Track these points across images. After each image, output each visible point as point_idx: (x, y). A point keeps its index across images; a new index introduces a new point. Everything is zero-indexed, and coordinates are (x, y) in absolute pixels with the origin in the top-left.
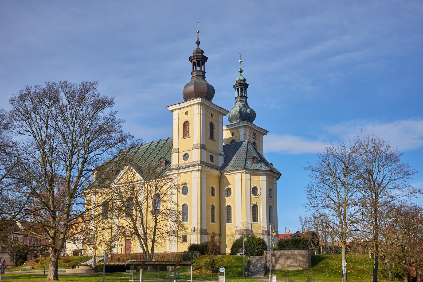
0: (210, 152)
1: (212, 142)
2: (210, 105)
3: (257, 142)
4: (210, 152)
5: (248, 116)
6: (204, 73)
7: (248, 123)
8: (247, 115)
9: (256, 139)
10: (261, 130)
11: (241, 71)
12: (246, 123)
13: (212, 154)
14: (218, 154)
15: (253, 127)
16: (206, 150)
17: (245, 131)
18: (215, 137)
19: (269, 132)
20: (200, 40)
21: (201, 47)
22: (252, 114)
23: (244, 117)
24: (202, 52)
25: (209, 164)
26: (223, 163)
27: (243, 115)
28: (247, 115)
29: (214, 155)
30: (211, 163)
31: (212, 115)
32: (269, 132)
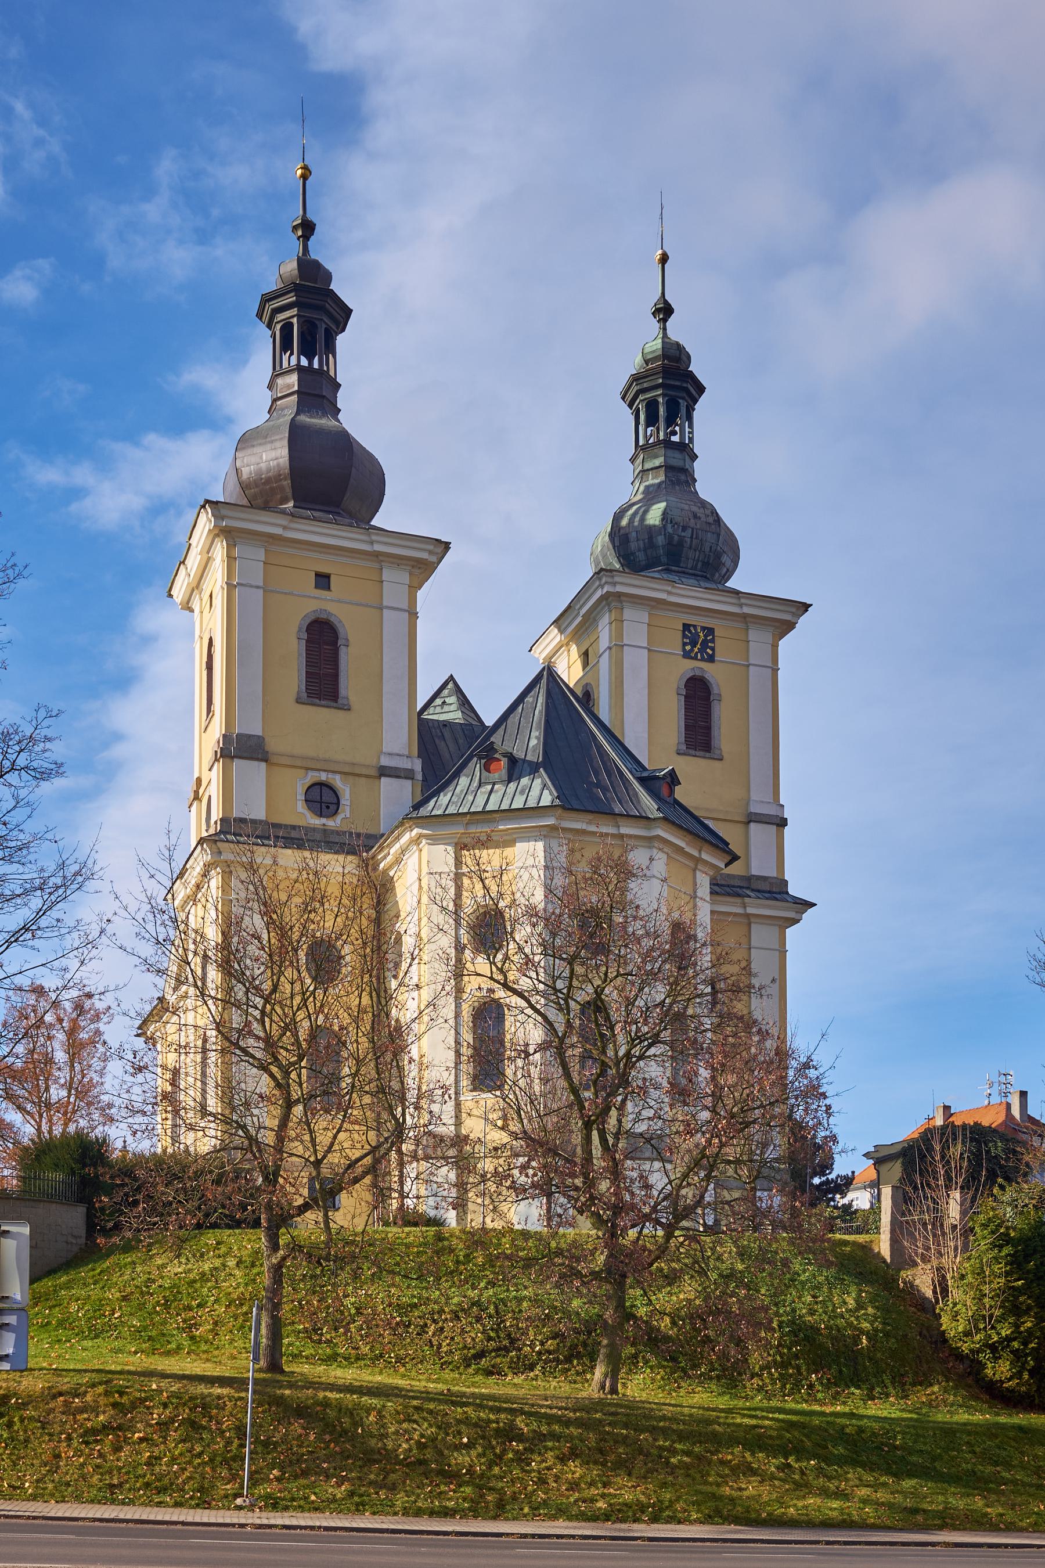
0: (307, 769)
1: (322, 715)
3: (712, 672)
4: (307, 769)
5: (660, 540)
8: (650, 538)
9: (711, 659)
10: (741, 606)
13: (323, 777)
14: (373, 772)
15: (669, 593)
16: (266, 760)
18: (351, 684)
19: (806, 607)
22: (684, 529)
23: (641, 556)
25: (294, 827)
27: (633, 546)
28: (650, 538)
29: (337, 781)
30: (316, 821)
32: (806, 607)
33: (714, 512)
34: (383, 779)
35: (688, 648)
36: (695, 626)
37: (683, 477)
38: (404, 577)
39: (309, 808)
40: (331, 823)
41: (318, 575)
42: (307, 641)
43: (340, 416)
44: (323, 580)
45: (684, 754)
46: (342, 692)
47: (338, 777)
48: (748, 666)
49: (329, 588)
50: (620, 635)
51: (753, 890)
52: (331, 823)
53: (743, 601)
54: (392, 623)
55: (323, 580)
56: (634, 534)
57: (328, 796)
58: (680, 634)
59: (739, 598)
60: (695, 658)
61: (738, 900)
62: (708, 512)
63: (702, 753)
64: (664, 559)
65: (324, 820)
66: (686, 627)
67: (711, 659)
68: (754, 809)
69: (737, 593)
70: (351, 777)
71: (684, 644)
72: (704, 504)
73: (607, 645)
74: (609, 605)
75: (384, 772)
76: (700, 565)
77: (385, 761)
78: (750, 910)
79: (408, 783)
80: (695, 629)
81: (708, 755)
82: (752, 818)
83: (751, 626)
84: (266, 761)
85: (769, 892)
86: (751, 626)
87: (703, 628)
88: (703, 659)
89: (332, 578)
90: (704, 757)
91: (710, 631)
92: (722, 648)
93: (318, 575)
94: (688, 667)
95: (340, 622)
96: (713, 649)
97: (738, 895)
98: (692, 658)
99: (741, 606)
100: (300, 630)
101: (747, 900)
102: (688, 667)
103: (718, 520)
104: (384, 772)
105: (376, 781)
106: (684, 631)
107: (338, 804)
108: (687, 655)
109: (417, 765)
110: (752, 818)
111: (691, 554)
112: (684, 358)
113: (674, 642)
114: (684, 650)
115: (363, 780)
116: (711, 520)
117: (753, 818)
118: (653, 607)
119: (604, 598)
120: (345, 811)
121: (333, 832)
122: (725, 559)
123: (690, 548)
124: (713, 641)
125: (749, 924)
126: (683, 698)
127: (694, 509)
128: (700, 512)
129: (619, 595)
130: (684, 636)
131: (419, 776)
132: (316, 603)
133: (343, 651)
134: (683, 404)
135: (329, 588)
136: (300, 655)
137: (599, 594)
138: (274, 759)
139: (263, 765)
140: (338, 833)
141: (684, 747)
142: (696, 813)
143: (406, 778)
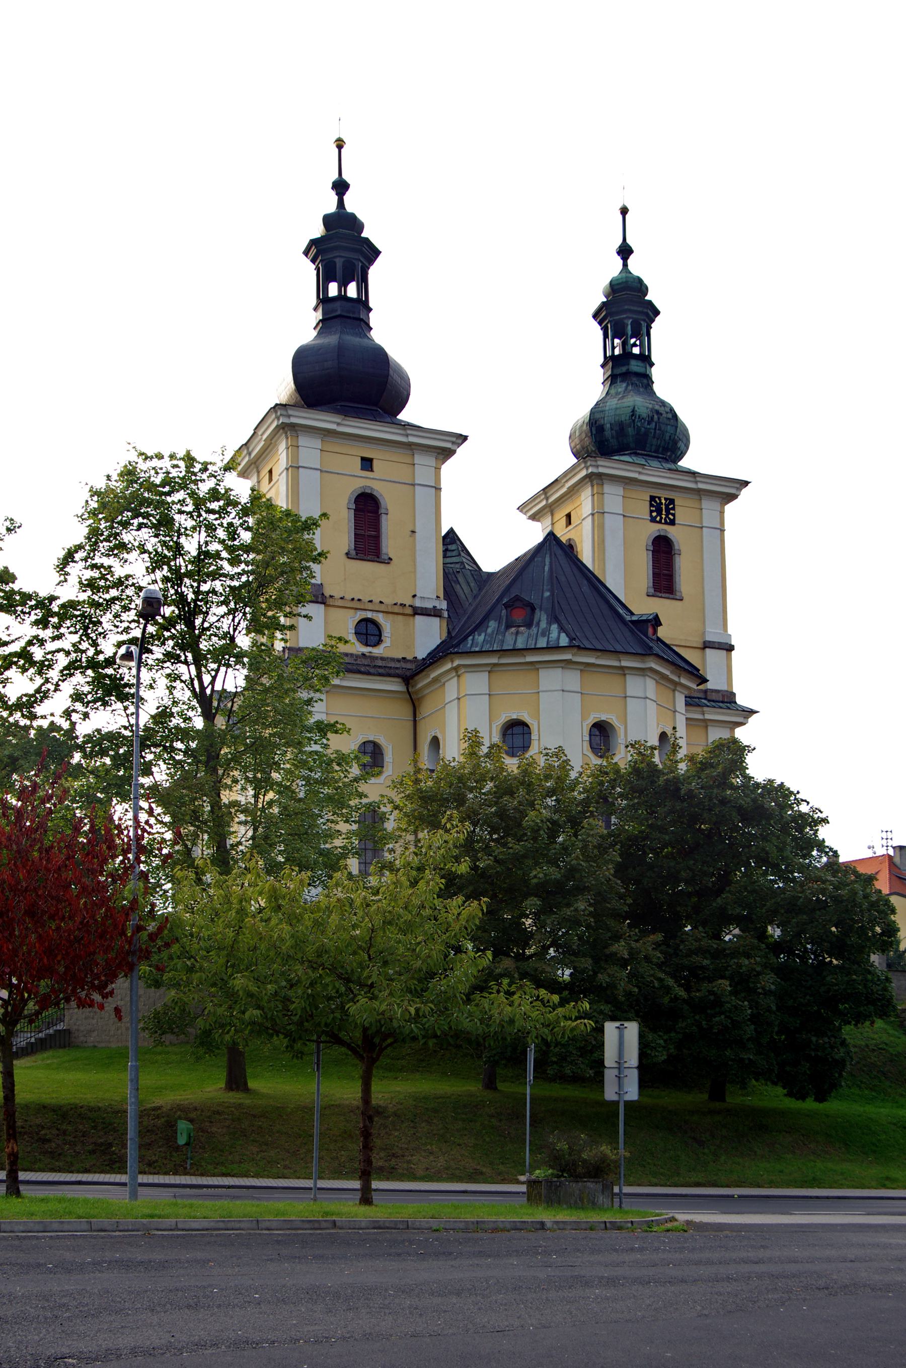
2: (338, 424)
3: (672, 532)
5: (630, 431)
6: (363, 304)
7: (600, 463)
10: (696, 482)
11: (625, 251)
12: (589, 464)
13: (369, 615)
14: (409, 611)
15: (640, 473)
16: (323, 603)
17: (599, 496)
18: (391, 543)
26: (439, 642)
27: (608, 433)
29: (380, 618)
33: (672, 410)
34: (418, 618)
35: (654, 514)
36: (660, 498)
37: (645, 381)
38: (430, 461)
39: (358, 640)
40: (377, 651)
41: (363, 459)
42: (355, 510)
44: (367, 464)
45: (653, 596)
46: (384, 549)
47: (380, 615)
48: (702, 528)
49: (372, 471)
50: (602, 503)
51: (709, 701)
52: (377, 651)
53: (698, 479)
55: (367, 464)
56: (608, 426)
57: (372, 629)
58: (648, 503)
59: (695, 477)
60: (660, 522)
61: (699, 709)
62: (668, 410)
63: (667, 595)
64: (632, 445)
65: (369, 649)
66: (652, 498)
67: (672, 523)
68: (709, 638)
69: (693, 474)
70: (390, 616)
71: (651, 512)
72: (663, 403)
73: (590, 512)
74: (591, 481)
75: (418, 611)
76: (661, 450)
77: (418, 603)
78: (707, 717)
79: (436, 620)
80: (660, 498)
81: (671, 596)
82: (707, 645)
83: (703, 497)
84: (324, 603)
85: (723, 702)
86: (703, 497)
87: (666, 499)
88: (666, 523)
89: (375, 462)
90: (668, 598)
91: (672, 501)
92: (681, 513)
93: (363, 459)
94: (655, 529)
95: (381, 495)
96: (674, 515)
97: (699, 706)
98: (657, 522)
99: (696, 482)
100: (349, 501)
101: (705, 709)
102: (655, 529)
103: (675, 416)
104: (418, 611)
105: (411, 618)
106: (650, 502)
107: (380, 635)
108: (653, 520)
109: (444, 605)
110: (707, 645)
111: (654, 442)
112: (644, 288)
113: (643, 509)
114: (651, 516)
115: (400, 617)
116: (670, 416)
117: (707, 645)
118: (626, 484)
119: (586, 476)
120: (387, 642)
121: (377, 658)
122: (681, 445)
123: (654, 437)
124: (673, 509)
125: (706, 727)
126: (650, 553)
127: (657, 407)
128: (662, 410)
129: (600, 476)
130: (651, 505)
131: (446, 614)
132: (361, 482)
133: (383, 517)
134: (644, 325)
135: (372, 471)
136: (349, 521)
137: (584, 473)
138: (330, 602)
139: (322, 606)
140: (382, 659)
141: (652, 591)
142: (668, 642)
143: (435, 616)
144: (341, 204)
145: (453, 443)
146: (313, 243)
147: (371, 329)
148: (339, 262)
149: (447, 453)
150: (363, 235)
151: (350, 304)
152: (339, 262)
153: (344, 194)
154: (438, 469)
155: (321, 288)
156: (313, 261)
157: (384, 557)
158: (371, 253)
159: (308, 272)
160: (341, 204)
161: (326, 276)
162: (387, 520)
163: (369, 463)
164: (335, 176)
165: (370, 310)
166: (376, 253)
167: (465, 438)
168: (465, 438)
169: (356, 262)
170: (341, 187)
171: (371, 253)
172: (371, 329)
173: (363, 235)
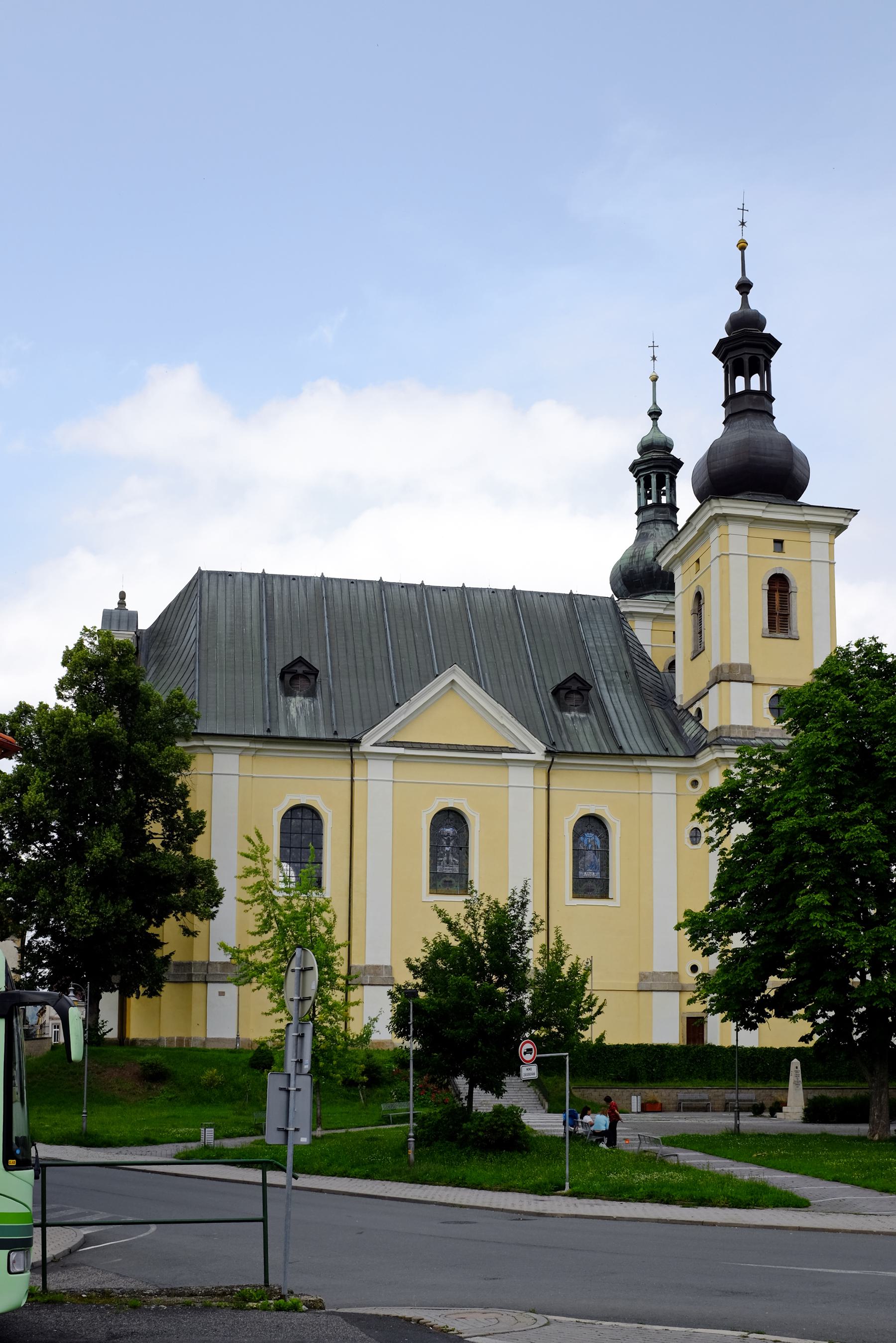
6: (766, 396)
20: (750, 276)
21: (756, 302)
24: (758, 321)
31: (779, 543)
38: (824, 536)
41: (776, 541)
43: (775, 422)
54: (818, 572)
133: (792, 595)
144: (745, 302)
145: (846, 519)
146: (722, 342)
147: (774, 418)
148: (746, 359)
149: (840, 529)
150: (766, 331)
151: (755, 397)
152: (746, 359)
153: (748, 293)
154: (831, 544)
155: (729, 383)
156: (722, 360)
157: (794, 634)
158: (772, 345)
159: (717, 367)
160: (745, 302)
161: (734, 369)
162: (796, 598)
163: (779, 545)
164: (739, 276)
165: (772, 399)
166: (777, 345)
167: (855, 512)
168: (855, 512)
169: (760, 357)
170: (744, 287)
171: (772, 345)
172: (774, 418)
173: (766, 331)
